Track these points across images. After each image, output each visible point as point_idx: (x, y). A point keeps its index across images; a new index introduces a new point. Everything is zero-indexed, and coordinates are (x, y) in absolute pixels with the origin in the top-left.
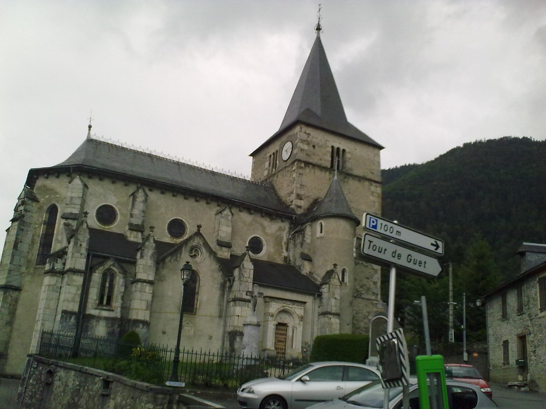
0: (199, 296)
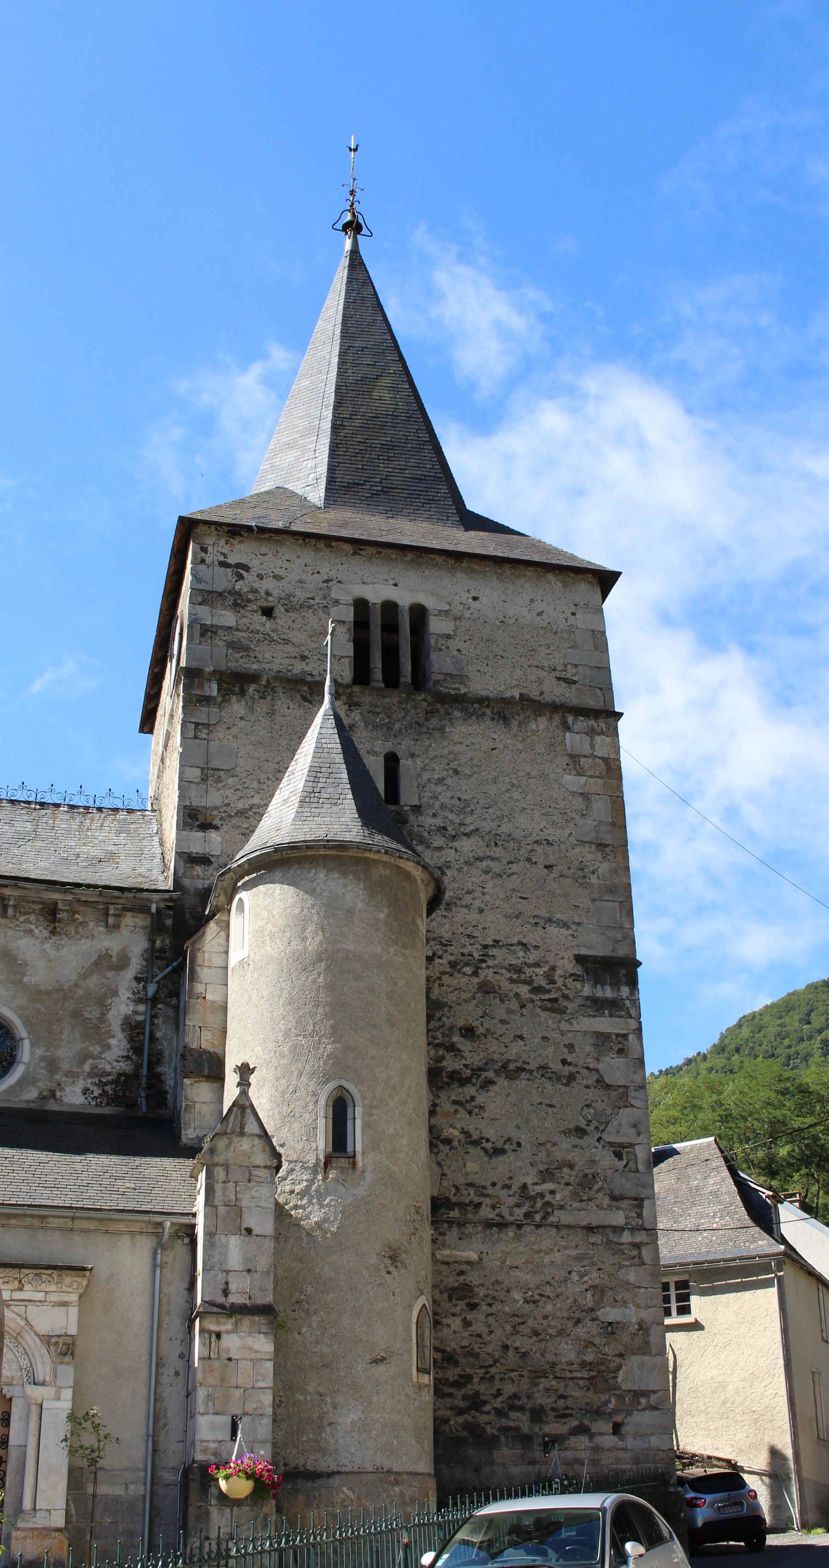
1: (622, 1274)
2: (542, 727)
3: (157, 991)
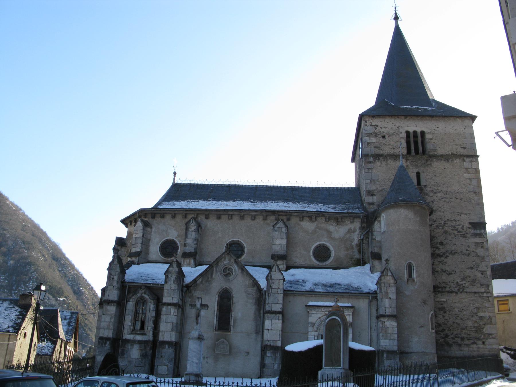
0: (233, 313)
1: (484, 304)
2: (458, 161)
3: (363, 238)
